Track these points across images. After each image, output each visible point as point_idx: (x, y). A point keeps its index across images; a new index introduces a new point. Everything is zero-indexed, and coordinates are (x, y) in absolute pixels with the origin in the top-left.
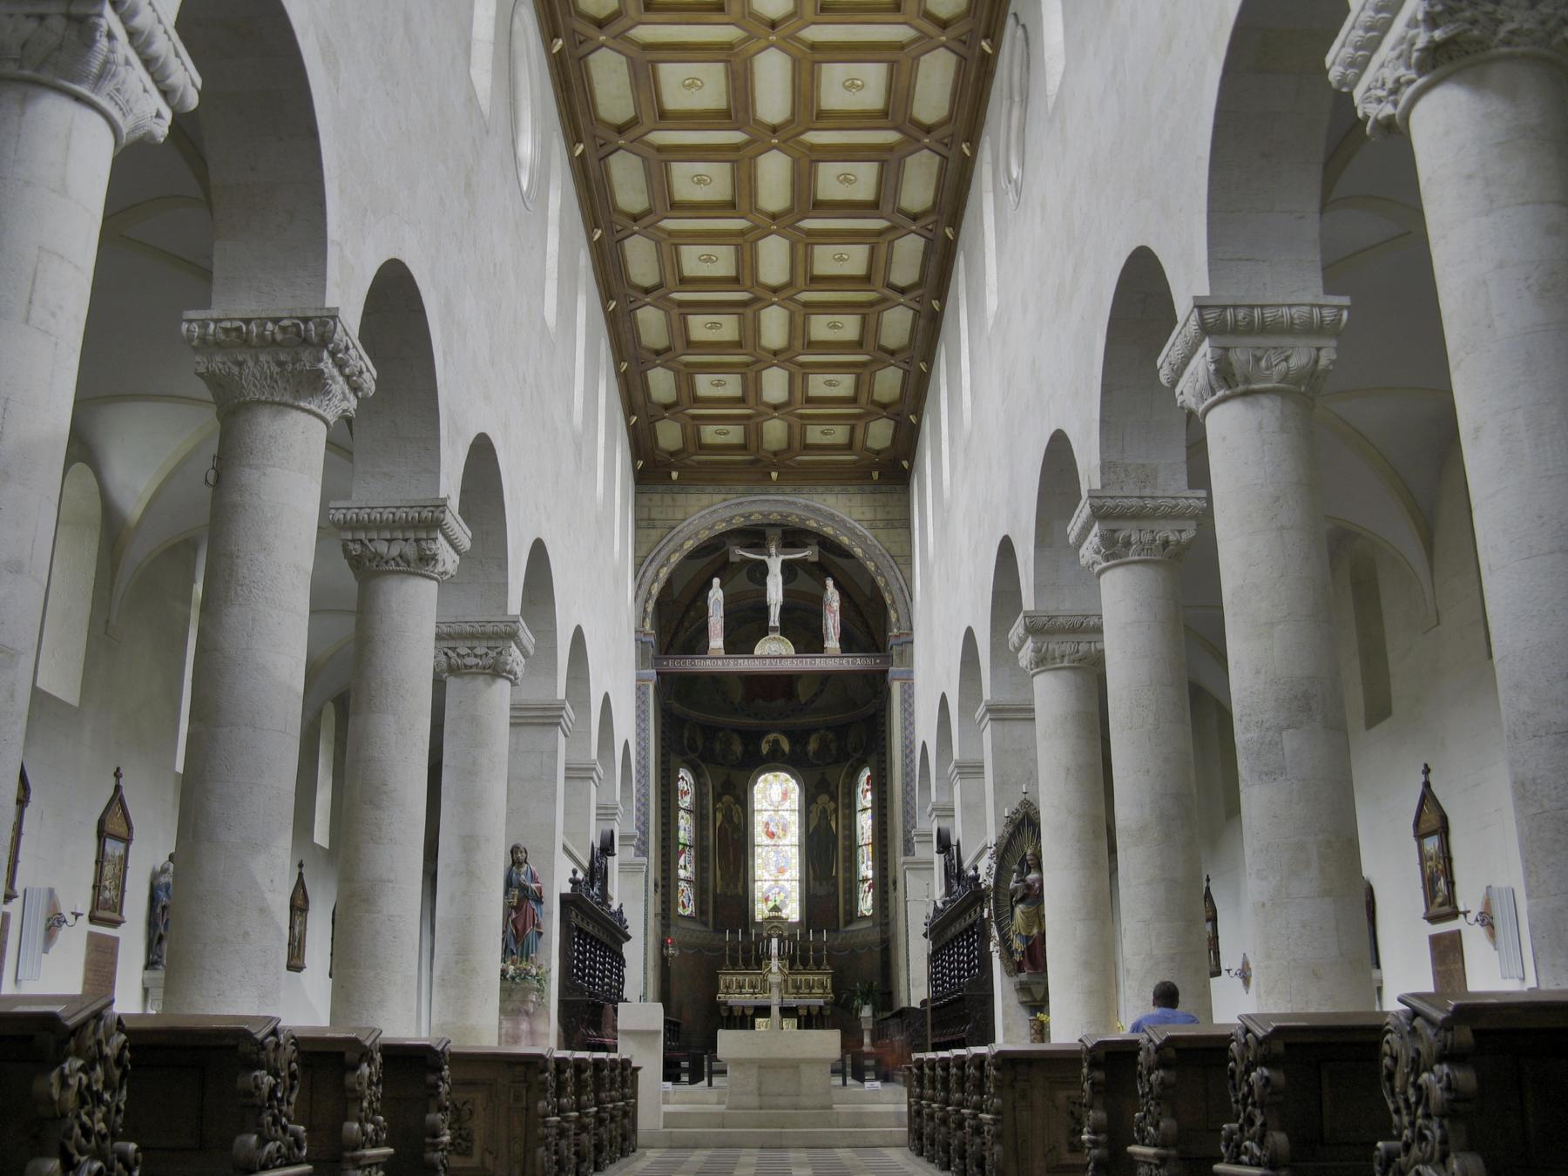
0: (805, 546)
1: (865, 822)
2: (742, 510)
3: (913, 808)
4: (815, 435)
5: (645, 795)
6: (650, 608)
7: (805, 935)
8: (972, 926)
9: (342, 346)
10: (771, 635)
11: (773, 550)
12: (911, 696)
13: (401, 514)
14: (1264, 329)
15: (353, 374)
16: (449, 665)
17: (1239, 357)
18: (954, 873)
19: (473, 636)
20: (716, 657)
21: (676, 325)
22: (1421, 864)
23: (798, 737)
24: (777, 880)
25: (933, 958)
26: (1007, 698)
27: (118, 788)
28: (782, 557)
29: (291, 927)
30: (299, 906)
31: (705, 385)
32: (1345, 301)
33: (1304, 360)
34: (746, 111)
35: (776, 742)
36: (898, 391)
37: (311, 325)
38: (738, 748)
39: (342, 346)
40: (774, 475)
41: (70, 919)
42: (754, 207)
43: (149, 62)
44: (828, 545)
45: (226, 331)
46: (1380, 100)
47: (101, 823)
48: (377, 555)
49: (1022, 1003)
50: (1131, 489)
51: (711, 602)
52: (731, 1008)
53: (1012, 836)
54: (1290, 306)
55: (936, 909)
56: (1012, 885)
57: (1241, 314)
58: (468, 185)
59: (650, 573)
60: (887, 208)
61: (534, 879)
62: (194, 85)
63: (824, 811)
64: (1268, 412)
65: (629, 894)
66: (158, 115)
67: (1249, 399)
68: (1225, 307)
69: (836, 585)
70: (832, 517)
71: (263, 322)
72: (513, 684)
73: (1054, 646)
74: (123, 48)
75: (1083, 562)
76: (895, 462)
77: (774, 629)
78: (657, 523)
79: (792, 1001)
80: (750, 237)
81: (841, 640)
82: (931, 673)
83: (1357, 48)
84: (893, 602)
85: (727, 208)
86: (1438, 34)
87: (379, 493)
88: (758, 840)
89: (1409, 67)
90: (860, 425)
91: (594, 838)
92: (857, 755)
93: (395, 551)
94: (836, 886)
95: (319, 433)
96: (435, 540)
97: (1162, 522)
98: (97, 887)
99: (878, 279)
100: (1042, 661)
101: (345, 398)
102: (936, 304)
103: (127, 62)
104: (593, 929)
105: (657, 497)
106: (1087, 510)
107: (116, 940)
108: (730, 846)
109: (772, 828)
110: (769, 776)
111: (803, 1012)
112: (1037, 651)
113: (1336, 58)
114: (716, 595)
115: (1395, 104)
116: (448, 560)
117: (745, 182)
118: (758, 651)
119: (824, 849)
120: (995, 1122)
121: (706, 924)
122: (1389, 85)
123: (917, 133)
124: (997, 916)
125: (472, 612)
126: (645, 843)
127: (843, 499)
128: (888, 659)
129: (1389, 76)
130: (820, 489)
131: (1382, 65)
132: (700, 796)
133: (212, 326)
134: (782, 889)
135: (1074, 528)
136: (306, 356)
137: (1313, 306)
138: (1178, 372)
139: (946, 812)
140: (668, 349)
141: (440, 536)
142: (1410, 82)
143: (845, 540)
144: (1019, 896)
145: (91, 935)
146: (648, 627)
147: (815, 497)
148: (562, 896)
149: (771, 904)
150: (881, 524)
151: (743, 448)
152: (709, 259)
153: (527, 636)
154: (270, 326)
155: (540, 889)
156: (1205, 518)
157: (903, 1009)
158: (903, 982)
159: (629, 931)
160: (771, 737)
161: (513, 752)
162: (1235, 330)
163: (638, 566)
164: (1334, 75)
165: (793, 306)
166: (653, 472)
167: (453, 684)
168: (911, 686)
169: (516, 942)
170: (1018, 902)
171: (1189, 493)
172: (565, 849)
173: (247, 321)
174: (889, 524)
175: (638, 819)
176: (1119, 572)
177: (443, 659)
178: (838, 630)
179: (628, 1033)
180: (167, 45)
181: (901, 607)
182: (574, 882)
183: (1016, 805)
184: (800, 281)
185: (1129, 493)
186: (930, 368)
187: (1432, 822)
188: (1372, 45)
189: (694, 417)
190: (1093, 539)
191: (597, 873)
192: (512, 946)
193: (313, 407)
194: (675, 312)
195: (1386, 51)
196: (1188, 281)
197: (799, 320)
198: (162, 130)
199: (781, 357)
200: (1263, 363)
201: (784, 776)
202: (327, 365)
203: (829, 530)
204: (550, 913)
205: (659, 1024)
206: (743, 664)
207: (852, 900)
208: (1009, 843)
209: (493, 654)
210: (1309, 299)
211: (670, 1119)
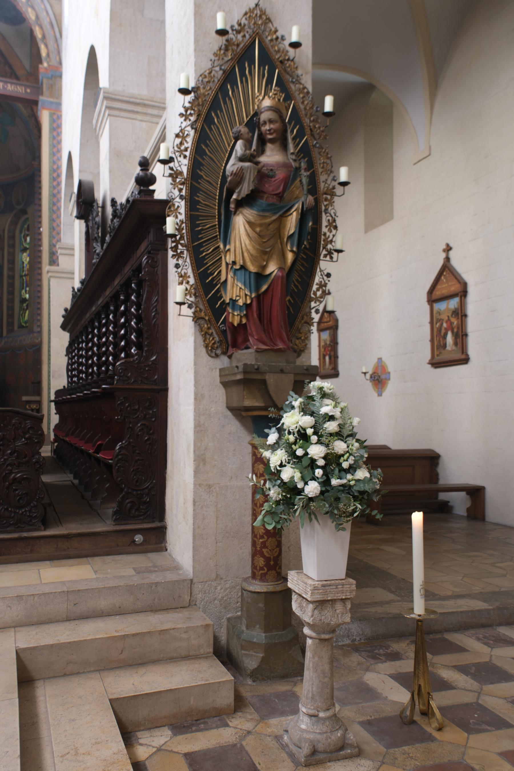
12: (59, 126)
49: (231, 409)
53: (229, 77)
84: (44, 37)
92: (20, 207)
128: (38, 89)
144: (245, 189)
168: (60, 117)
170: (240, 204)
208: (222, 89)
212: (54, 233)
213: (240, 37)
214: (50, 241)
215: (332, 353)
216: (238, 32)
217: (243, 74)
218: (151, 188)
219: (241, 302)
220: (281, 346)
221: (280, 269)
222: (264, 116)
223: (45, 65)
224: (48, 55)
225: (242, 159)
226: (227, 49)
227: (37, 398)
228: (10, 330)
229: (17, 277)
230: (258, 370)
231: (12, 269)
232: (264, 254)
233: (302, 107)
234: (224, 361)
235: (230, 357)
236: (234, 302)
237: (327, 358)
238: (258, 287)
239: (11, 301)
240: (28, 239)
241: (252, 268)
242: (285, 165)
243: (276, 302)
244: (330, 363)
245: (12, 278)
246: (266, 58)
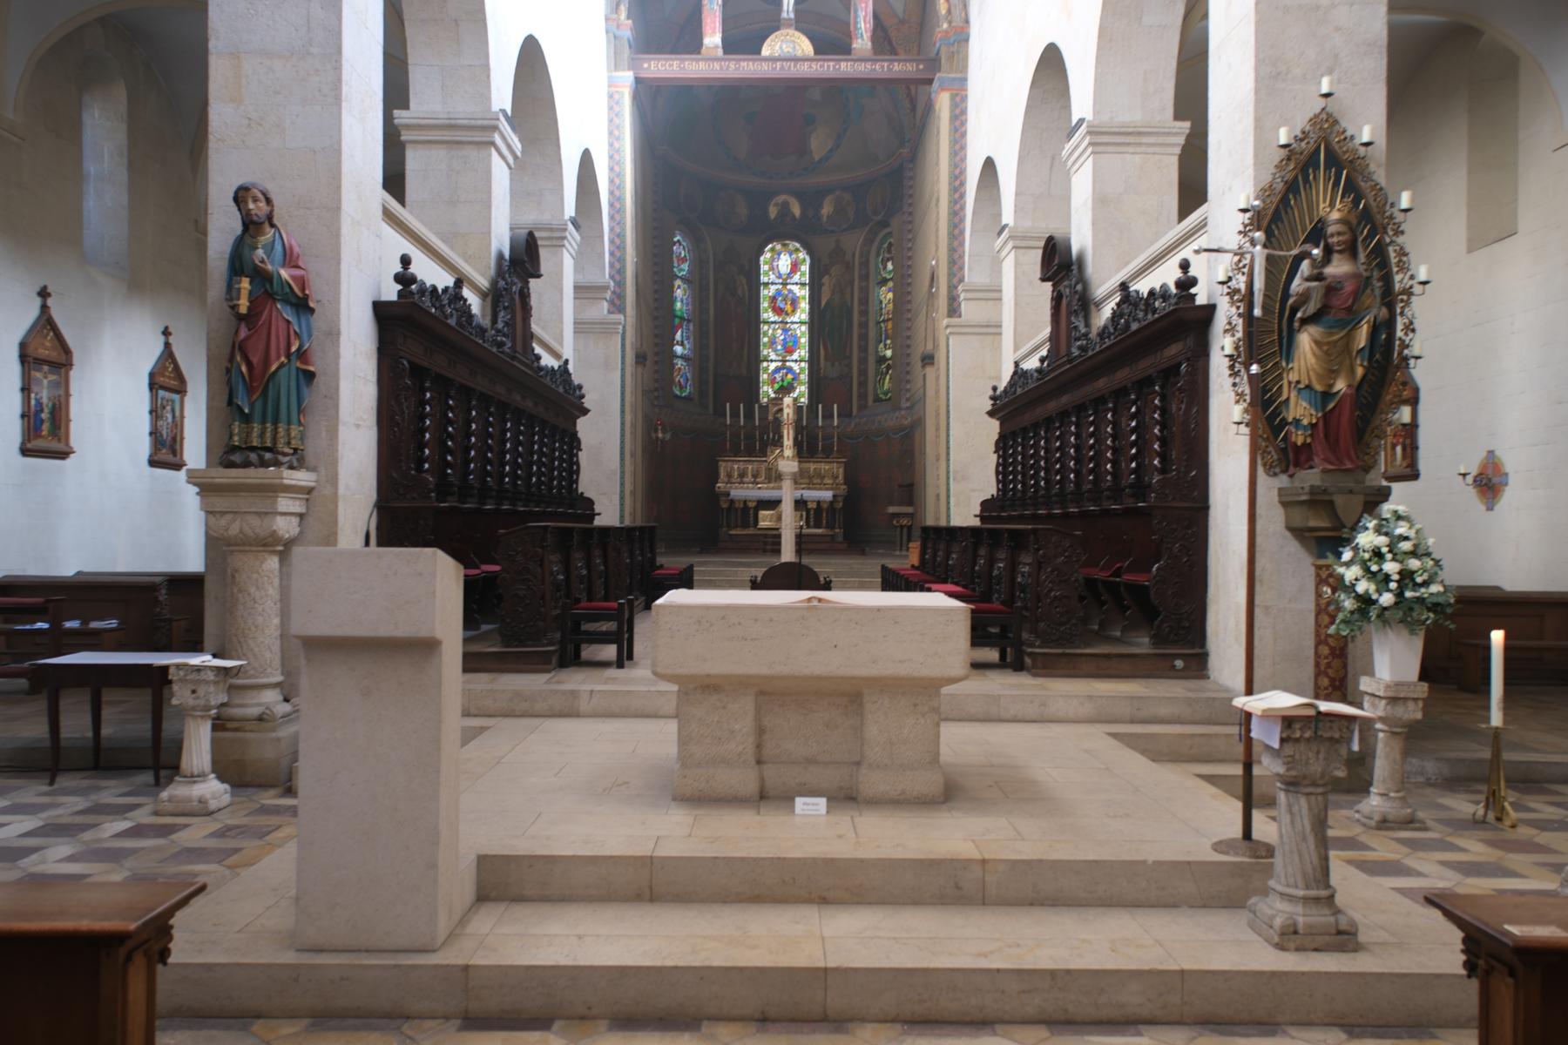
3: (962, 257)
12: (964, 112)
20: (710, 61)
23: (810, 200)
25: (1002, 444)
29: (26, 390)
35: (785, 205)
49: (1291, 529)
52: (732, 501)
53: (1292, 188)
55: (1019, 375)
56: (1297, 285)
61: (290, 259)
81: (874, 39)
88: (764, 316)
91: (500, 240)
92: (879, 217)
94: (849, 366)
111: (810, 505)
118: (766, 51)
128: (934, 64)
132: (699, 263)
134: (790, 370)
144: (1311, 308)
146: (623, 16)
148: (381, 310)
149: (776, 386)
155: (303, 283)
159: (587, 403)
160: (781, 198)
168: (964, 99)
169: (250, 390)
170: (1305, 321)
175: (612, 265)
182: (404, 279)
183: (1301, 122)
192: (242, 401)
206: (744, 68)
208: (1284, 200)
212: (955, 269)
213: (1303, 144)
214: (949, 281)
215: (1408, 441)
216: (1302, 140)
217: (1306, 181)
218: (1193, 291)
219: (1305, 422)
220: (1349, 465)
221: (1349, 386)
222: (1331, 229)
223: (945, 26)
224: (949, 11)
225: (1308, 279)
226: (1289, 159)
227: (910, 510)
228: (863, 407)
229: (872, 324)
230: (1325, 491)
231: (864, 313)
233: (1374, 204)
235: (1291, 476)
236: (1297, 422)
237: (1399, 449)
238: (1324, 406)
239: (863, 361)
240: (890, 266)
241: (1318, 387)
242: (1355, 276)
243: (1345, 419)
244: (1404, 457)
245: (864, 325)
246: (1334, 161)
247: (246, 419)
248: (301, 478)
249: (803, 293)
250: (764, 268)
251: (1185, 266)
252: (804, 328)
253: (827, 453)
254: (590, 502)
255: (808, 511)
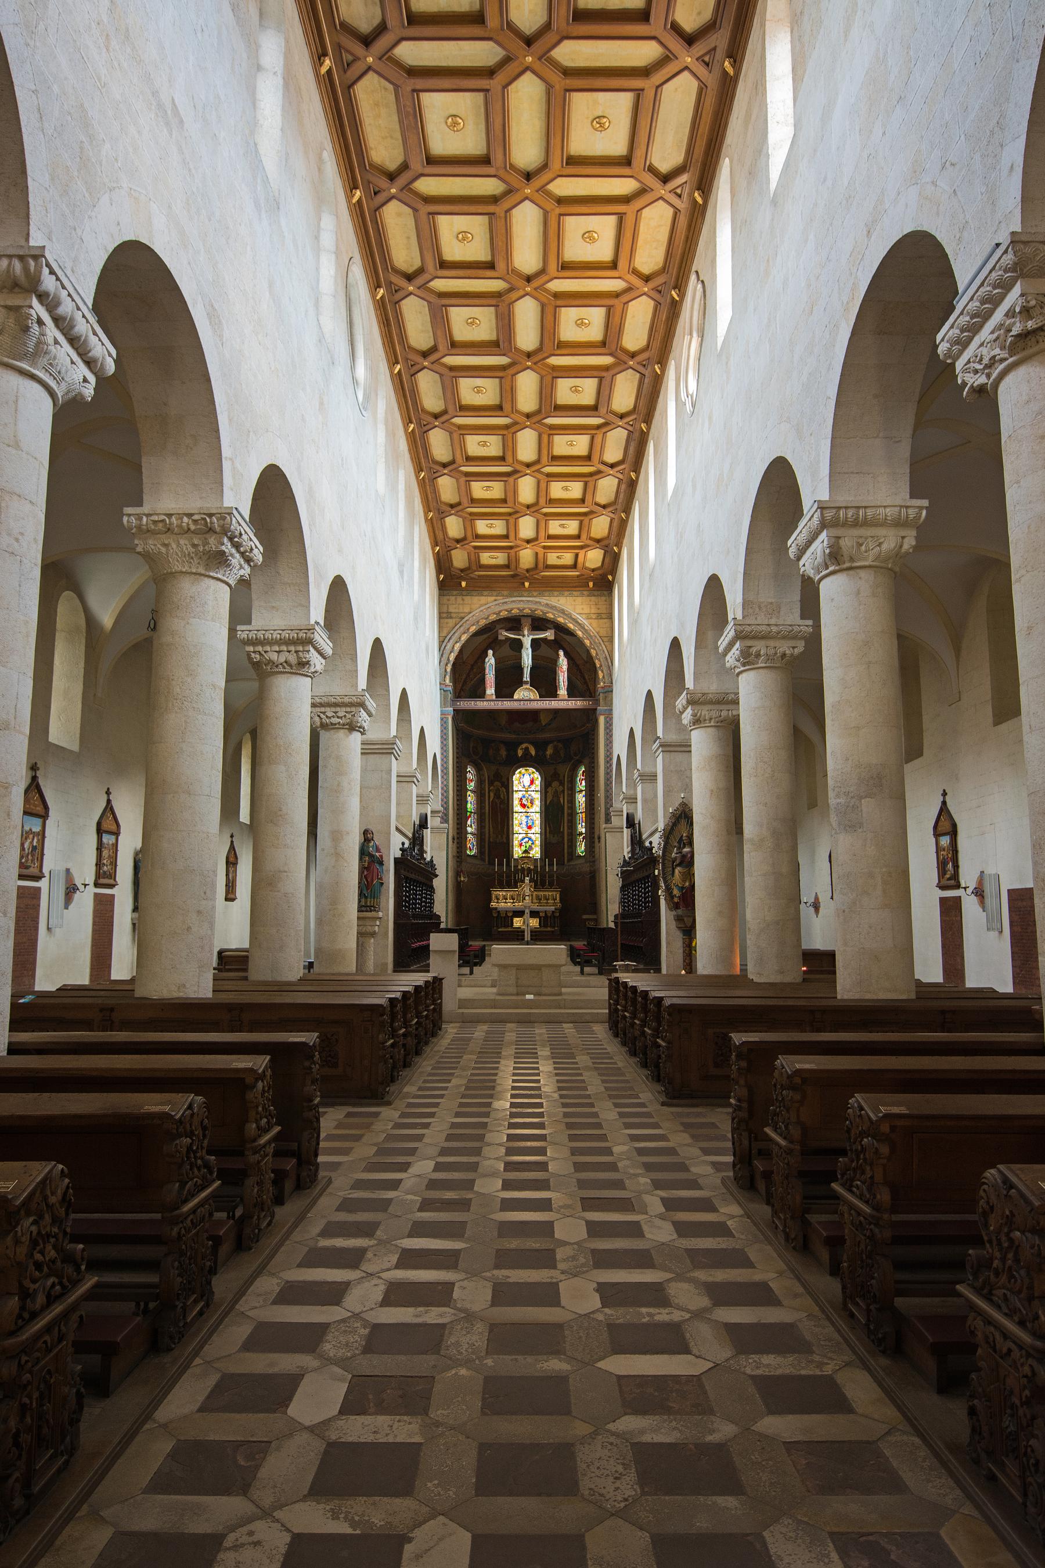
0: (544, 629)
1: (581, 799)
2: (506, 607)
4: (552, 558)
5: (447, 786)
6: (449, 670)
7: (543, 867)
8: (648, 877)
9: (237, 533)
10: (525, 686)
11: (526, 632)
13: (285, 634)
14: (866, 523)
15: (246, 551)
16: (321, 723)
17: (846, 544)
18: (637, 841)
19: (336, 705)
20: (490, 700)
21: (463, 488)
22: (937, 852)
23: (541, 746)
24: (527, 832)
25: (623, 889)
26: (673, 737)
27: (109, 801)
28: (531, 637)
29: (227, 875)
30: (232, 862)
31: (482, 527)
32: (925, 503)
33: (893, 545)
34: (510, 343)
35: (527, 749)
36: (606, 531)
37: (214, 519)
38: (503, 753)
39: (237, 533)
40: (527, 584)
41: (81, 888)
42: (514, 410)
43: (74, 341)
44: (560, 628)
45: (155, 522)
46: (976, 372)
47: (99, 824)
48: (270, 661)
50: (762, 619)
51: (487, 666)
53: (674, 824)
54: (885, 507)
55: (625, 860)
57: (850, 513)
58: (321, 404)
59: (449, 647)
60: (603, 410)
61: (378, 850)
62: (110, 355)
63: (556, 791)
64: (865, 580)
65: (436, 849)
66: (85, 380)
67: (851, 572)
68: (839, 508)
69: (566, 655)
70: (563, 612)
71: (180, 516)
72: (362, 734)
73: (704, 711)
74: (52, 331)
75: (728, 665)
76: (604, 577)
77: (526, 683)
78: (454, 615)
79: (535, 907)
80: (512, 430)
82: (625, 715)
83: (962, 331)
85: (498, 409)
86: (1030, 324)
87: (269, 619)
89: (1003, 348)
90: (582, 553)
93: (282, 659)
95: (225, 593)
96: (308, 651)
97: (782, 642)
98: (99, 864)
99: (595, 458)
100: (697, 721)
101: (241, 567)
102: (633, 475)
103: (56, 342)
104: (414, 871)
105: (453, 598)
106: (732, 633)
107: (113, 896)
108: (497, 813)
109: (524, 802)
110: (522, 770)
112: (694, 715)
113: (945, 336)
114: (490, 660)
115: (988, 376)
116: (317, 662)
117: (508, 391)
118: (516, 697)
119: (556, 814)
120: (668, 1048)
121: (483, 860)
122: (986, 361)
123: (624, 358)
124: (664, 874)
125: (335, 688)
126: (446, 815)
127: (570, 599)
128: (597, 702)
129: (986, 353)
130: (556, 593)
131: (982, 345)
132: (480, 782)
133: (145, 519)
134: (530, 839)
135: (723, 643)
136: (212, 540)
137: (901, 507)
138: (802, 551)
139: (632, 800)
140: (459, 504)
141: (311, 649)
142: (1002, 360)
143: (571, 626)
144: (678, 862)
145: (96, 894)
146: (448, 681)
147: (553, 599)
149: (523, 848)
150: (594, 616)
151: (507, 567)
152: (484, 444)
153: (371, 704)
154: (185, 519)
155: (381, 856)
156: (814, 641)
157: (604, 929)
158: (603, 900)
159: (437, 872)
160: (524, 746)
161: (364, 770)
162: (845, 524)
163: (441, 643)
164: (943, 348)
165: (540, 476)
166: (450, 580)
167: (324, 735)
168: (611, 719)
171: (802, 622)
172: (397, 829)
173: (169, 516)
174: (599, 617)
176: (752, 674)
177: (317, 719)
178: (566, 684)
179: (436, 951)
180: (86, 325)
181: (605, 669)
184: (545, 459)
185: (760, 621)
186: (628, 517)
187: (946, 826)
188: (974, 329)
189: (475, 547)
190: (735, 651)
191: (417, 840)
192: (365, 892)
193: (219, 576)
194: (464, 479)
195: (985, 334)
196: (814, 487)
197: (543, 485)
198: (89, 392)
199: (533, 509)
200: (863, 548)
201: (531, 770)
202: (227, 547)
203: (561, 620)
204: (388, 871)
205: (456, 947)
206: (506, 705)
207: (572, 846)
208: (672, 829)
209: (349, 716)
210: (899, 502)
211: (463, 1003)
227: (594, 917)
232: (684, 881)
234: (674, 913)
247: (366, 897)
248: (380, 914)
249: (537, 796)
250: (515, 782)
251: (651, 843)
252: (538, 815)
253: (551, 885)
254: (439, 917)
255: (540, 918)
